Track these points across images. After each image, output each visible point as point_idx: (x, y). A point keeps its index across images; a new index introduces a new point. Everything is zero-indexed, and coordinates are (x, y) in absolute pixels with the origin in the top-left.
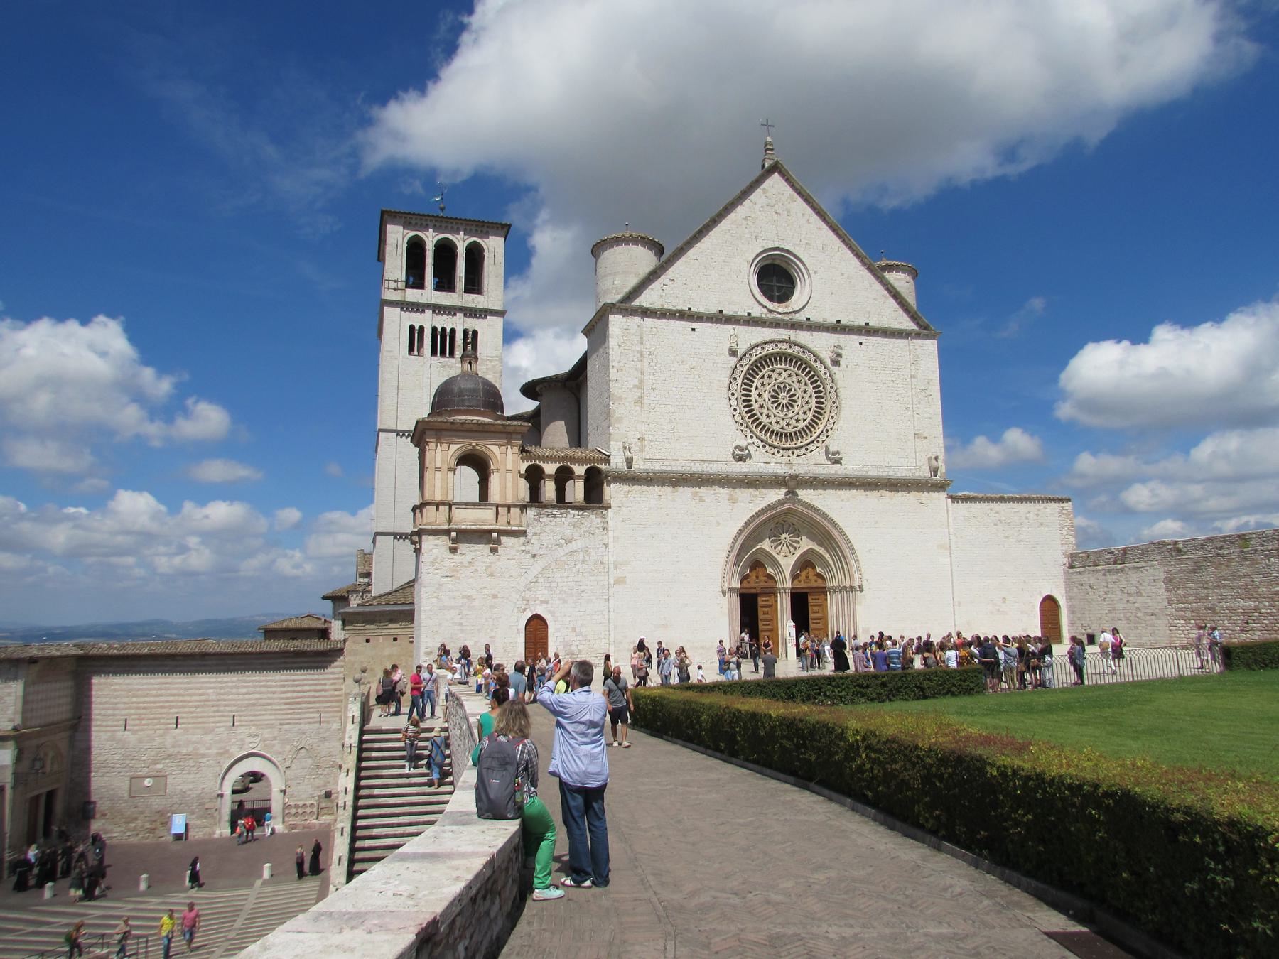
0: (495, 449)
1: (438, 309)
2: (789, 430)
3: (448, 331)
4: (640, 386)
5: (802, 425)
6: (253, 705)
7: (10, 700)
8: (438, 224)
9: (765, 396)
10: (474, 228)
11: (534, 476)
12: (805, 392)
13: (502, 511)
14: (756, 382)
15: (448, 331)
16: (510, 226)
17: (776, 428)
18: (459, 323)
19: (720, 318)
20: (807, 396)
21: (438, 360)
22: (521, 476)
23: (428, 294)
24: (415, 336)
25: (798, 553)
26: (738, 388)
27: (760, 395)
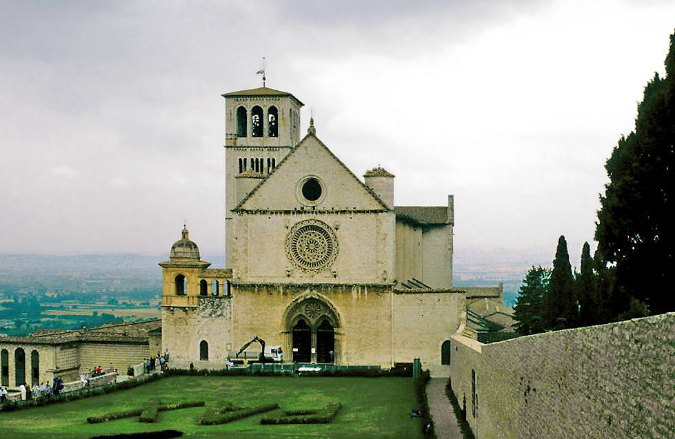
0: (187, 274)
2: (314, 261)
4: (246, 244)
5: (320, 259)
7: (51, 358)
11: (204, 285)
12: (323, 243)
13: (191, 299)
14: (299, 239)
17: (308, 260)
20: (323, 245)
22: (198, 284)
23: (250, 140)
25: (319, 316)
26: (291, 242)
27: (301, 246)
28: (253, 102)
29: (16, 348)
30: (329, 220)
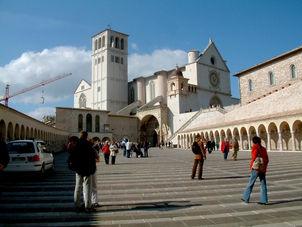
1: (117, 52)
2: (215, 85)
3: (118, 57)
5: (216, 84)
6: (125, 126)
7: (106, 119)
8: (116, 33)
9: (212, 79)
10: (123, 35)
14: (211, 77)
15: (118, 57)
16: (129, 36)
17: (213, 84)
18: (120, 56)
19: (207, 65)
21: (116, 63)
24: (112, 57)
28: (116, 35)
29: (87, 113)
30: (218, 71)
